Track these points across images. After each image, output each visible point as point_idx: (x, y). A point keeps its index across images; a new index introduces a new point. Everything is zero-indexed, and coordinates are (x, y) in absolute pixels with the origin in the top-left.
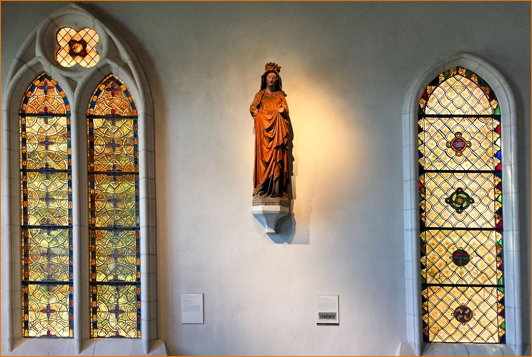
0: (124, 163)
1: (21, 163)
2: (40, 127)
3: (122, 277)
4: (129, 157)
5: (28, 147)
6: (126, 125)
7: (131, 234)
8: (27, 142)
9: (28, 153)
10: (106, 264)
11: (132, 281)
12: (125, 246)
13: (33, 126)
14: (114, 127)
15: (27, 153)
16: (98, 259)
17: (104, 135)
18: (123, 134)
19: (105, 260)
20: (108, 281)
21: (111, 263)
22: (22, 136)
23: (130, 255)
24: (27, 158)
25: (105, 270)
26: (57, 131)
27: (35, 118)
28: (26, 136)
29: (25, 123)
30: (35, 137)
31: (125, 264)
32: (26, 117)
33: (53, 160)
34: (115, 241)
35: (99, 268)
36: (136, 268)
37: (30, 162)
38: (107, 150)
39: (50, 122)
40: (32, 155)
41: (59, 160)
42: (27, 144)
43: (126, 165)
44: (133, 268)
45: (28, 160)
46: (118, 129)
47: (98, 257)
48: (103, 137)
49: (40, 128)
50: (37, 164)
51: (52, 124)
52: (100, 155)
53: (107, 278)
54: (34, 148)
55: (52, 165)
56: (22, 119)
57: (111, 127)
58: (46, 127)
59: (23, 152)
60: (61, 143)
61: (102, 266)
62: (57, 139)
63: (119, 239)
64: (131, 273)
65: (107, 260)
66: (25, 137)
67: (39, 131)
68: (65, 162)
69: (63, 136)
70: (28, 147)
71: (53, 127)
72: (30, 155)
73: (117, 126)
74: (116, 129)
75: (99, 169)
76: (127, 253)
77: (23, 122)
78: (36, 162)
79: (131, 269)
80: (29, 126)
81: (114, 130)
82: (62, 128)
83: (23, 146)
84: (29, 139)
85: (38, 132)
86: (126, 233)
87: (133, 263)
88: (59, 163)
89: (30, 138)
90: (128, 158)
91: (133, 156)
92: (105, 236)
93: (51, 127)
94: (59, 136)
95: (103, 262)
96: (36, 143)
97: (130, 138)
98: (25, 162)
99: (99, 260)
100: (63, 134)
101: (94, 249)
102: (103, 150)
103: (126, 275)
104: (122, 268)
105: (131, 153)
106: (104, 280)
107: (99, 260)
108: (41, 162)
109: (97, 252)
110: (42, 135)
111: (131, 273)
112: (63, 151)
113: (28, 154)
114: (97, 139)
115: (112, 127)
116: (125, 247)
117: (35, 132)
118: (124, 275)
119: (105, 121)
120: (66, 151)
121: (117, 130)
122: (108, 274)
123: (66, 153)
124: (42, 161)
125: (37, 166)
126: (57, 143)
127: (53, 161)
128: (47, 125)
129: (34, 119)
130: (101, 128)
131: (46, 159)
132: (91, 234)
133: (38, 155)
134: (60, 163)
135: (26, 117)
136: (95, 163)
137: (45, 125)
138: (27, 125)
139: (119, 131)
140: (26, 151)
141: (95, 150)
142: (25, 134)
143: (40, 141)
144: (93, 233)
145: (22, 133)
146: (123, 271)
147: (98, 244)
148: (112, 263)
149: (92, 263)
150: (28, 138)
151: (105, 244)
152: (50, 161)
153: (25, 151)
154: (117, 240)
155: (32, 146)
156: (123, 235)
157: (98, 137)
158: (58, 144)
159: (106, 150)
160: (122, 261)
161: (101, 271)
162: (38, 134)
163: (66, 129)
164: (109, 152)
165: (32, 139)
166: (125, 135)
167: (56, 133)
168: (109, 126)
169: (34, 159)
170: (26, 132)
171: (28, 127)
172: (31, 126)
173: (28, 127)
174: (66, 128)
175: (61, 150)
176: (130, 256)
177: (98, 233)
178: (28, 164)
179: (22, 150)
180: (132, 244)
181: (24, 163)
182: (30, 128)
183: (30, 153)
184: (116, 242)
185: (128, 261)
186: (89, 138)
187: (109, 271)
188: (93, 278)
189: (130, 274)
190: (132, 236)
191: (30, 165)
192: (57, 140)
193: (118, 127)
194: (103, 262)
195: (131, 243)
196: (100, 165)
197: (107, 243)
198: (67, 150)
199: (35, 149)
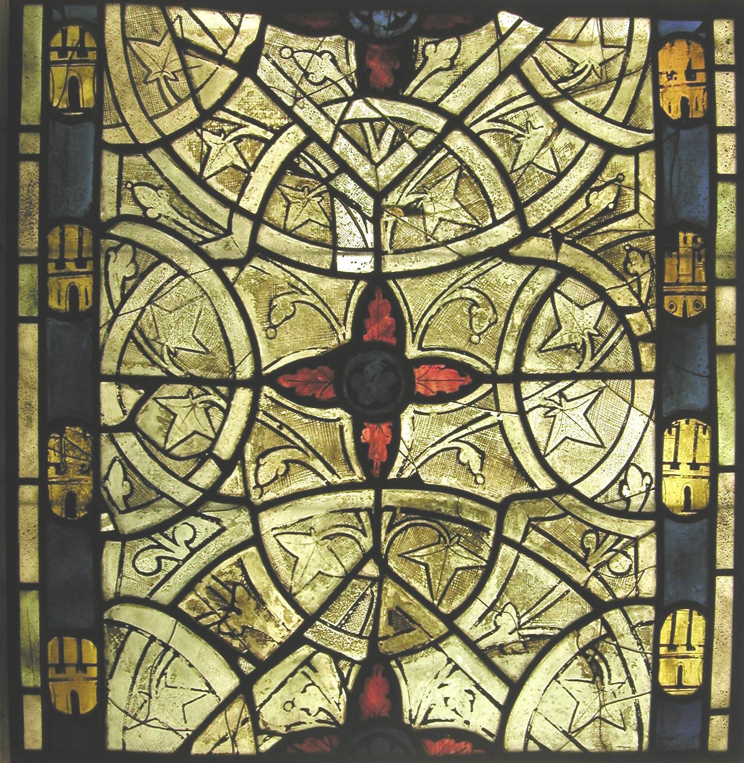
3: (457, 685)
7: (591, 56)
10: (242, 502)
11: (590, 745)
12: (508, 231)
16: (130, 425)
19: (225, 448)
20: (267, 745)
21: (309, 481)
23: (569, 365)
25: (231, 586)
31: (503, 508)
34: (364, 170)
35: (147, 563)
36: (648, 551)
44: (621, 564)
47: (131, 396)
53: (255, 715)
61: (183, 532)
63: (422, 140)
64: (589, 633)
65: (264, 438)
76: (536, 339)
79: (580, 576)
86: (517, 44)
87: (621, 480)
92: (234, 87)
95: (207, 475)
99: (144, 438)
101: (84, 284)
103: (514, 665)
104: (460, 559)
106: (217, 729)
107: (144, 438)
109: (125, 323)
111: (589, 633)
116: (502, 253)
118: (484, 656)
122: (264, 652)
132: (47, 65)
144: (63, 51)
146: (477, 608)
147: (128, 208)
148: (330, 488)
149: (42, 482)
151: (234, 208)
154: (393, 149)
156: (488, 71)
160: (469, 456)
161: (171, 609)
176: (574, 377)
177: (130, 56)
180: (603, 199)
184: (387, 172)
185: (541, 458)
187: (277, 605)
188: (62, 705)
189: (564, 651)
190: (604, 95)
194: (207, 475)
195: (587, 186)
197: (251, 203)
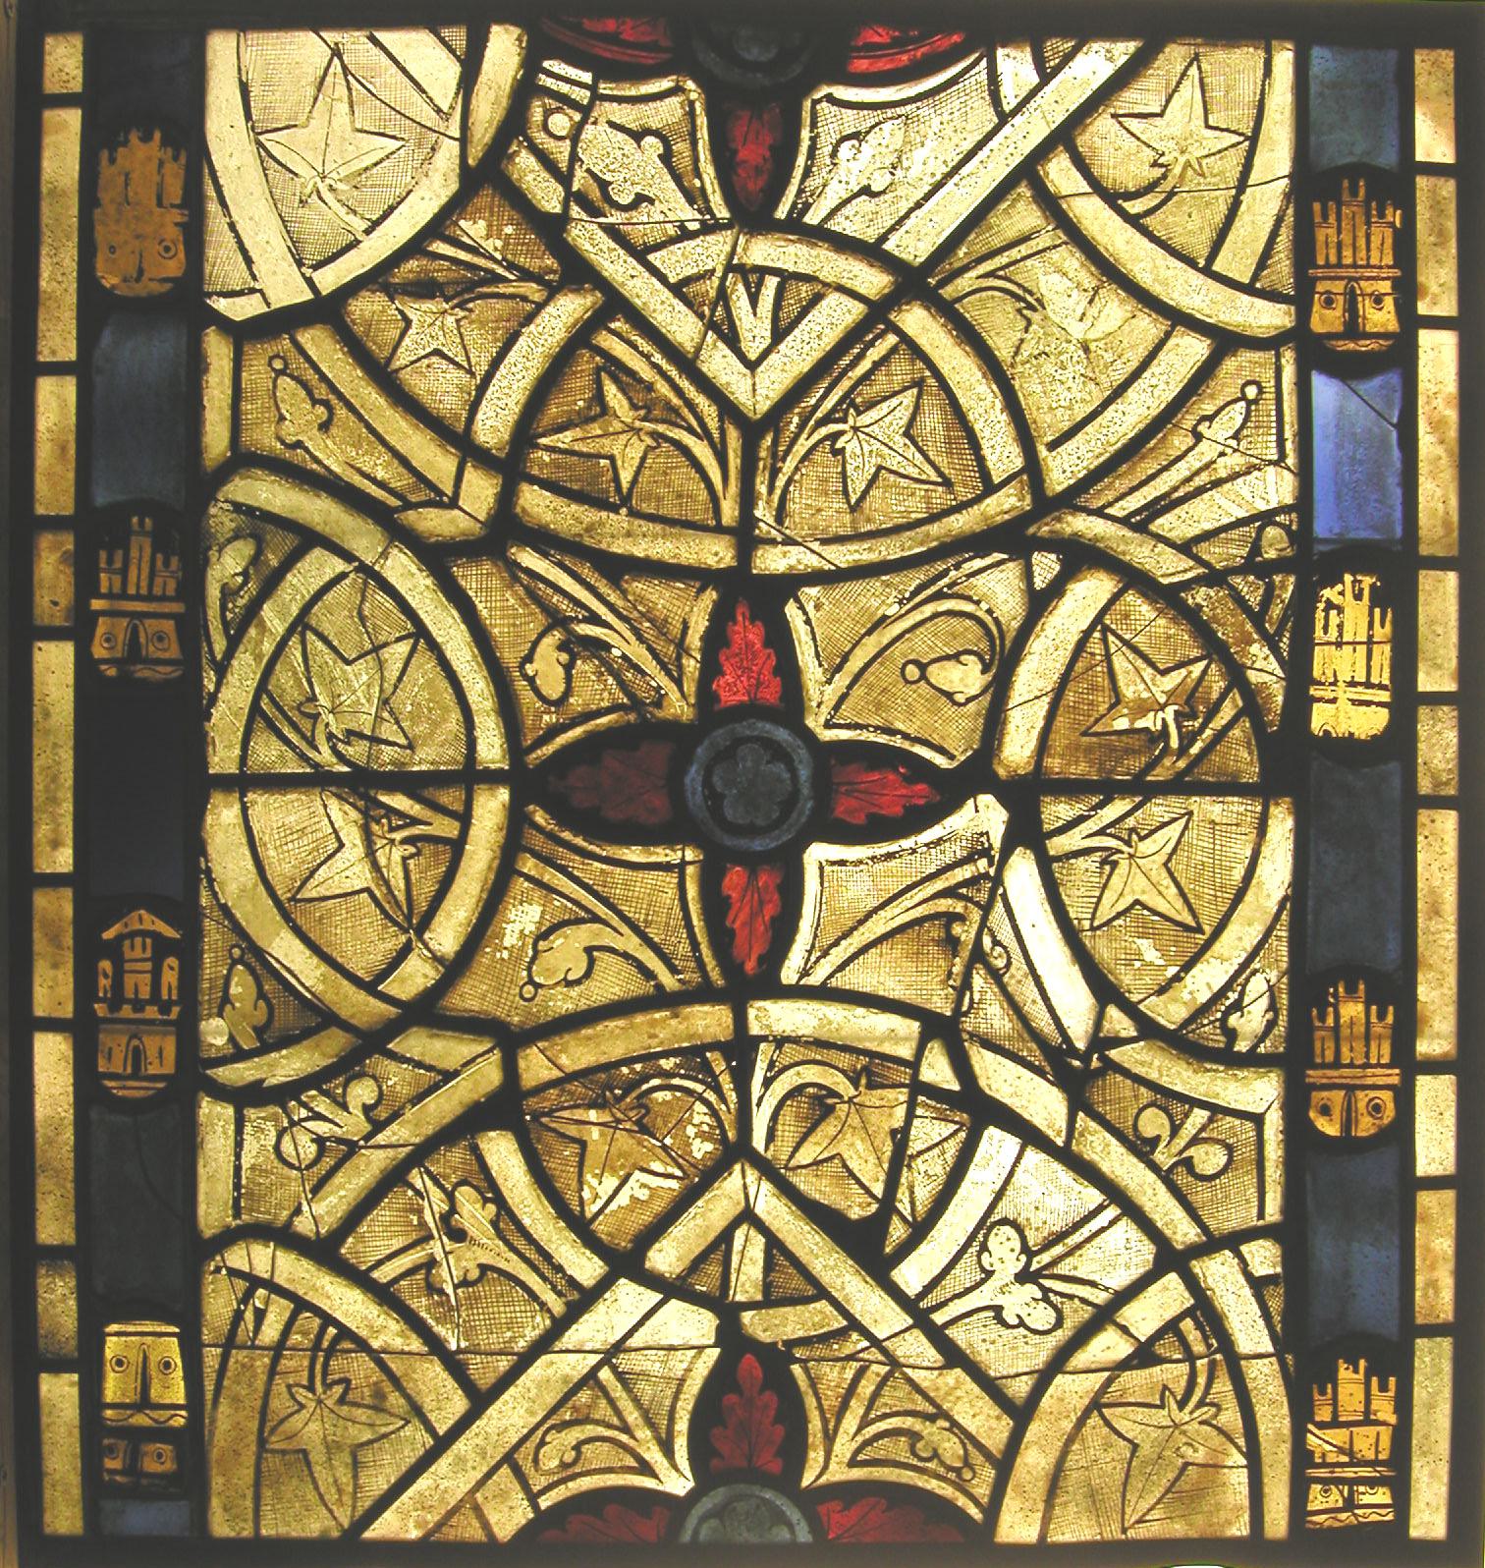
0: (1020, 1301)
4: (1153, 1123)
6: (1112, 198)
14: (762, 251)
17: (480, 492)
18: (1003, 455)
38: (568, 947)
43: (1058, 1363)
46: (878, 314)
48: (437, 557)
52: (362, 1092)
57: (676, 262)
73: (854, 224)
74: (835, 316)
75: (332, 1474)
81: (754, 328)
90: (1142, 1148)
91: (1261, 1092)
97: (1215, 578)
102: (447, 935)
105: (1227, 999)
114: (301, 624)
115: (711, 251)
119: (525, 90)
121: (855, 337)
130: (424, 289)
136: (218, 1302)
139: (902, 369)
141: (214, 934)
157: (319, 567)
159: (522, 918)
164: (613, 983)
166: (1062, 469)
168: (645, 225)
186: (85, 585)
193: (872, 252)
196: (360, 1369)
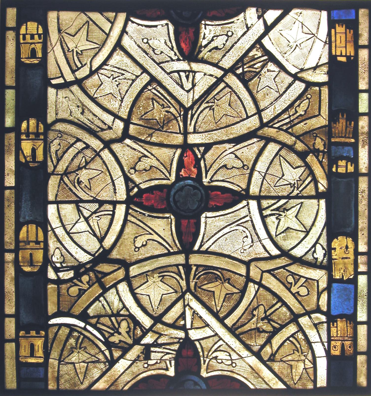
1: (10, 348)
2: (146, 78)
5: (60, 232)
8: (51, 197)
9: (57, 270)
13: (92, 73)
15: (51, 275)
22: (18, 149)
24: (52, 308)
26: (259, 112)
27: (111, 15)
28: (46, 150)
29: (40, 55)
30: (106, 154)
32: (52, 16)
33: (229, 322)
37: (72, 341)
39: (219, 42)
40: (82, 292)
41: (267, 318)
42: (52, 209)
45: (60, 325)
49: (145, 87)
50: (117, 354)
51: (227, 63)
54: (101, 240)
55: (221, 355)
56: (23, 31)
58: (188, 86)
59: (27, 269)
60: (289, 197)
62: (261, 166)
66: (40, 156)
67: (139, 111)
68: (313, 335)
69: (300, 146)
70: (60, 232)
71: (232, 80)
72: (74, 291)
77: (25, 51)
78: (115, 339)
80: (70, 77)
82: (299, 87)
83: (28, 223)
84: (66, 173)
85: (127, 122)
88: (269, 341)
89: (76, 162)
93: (220, 80)
94: (272, 148)
96: (114, 203)
98: (39, 343)
100: (300, 128)
108: (149, 339)
110: (154, 139)
112: (298, 252)
113: (59, 282)
117: (108, 119)
120: (320, 254)
123: (320, 267)
124: (150, 329)
125: (121, 366)
126: (259, 198)
127: (232, 330)
128: (195, 66)
129: (107, 26)
131: (183, 316)
133: (123, 287)
134: (277, 341)
135: (52, 16)
137: (183, 65)
138: (52, 70)
140: (47, 260)
142: (37, 134)
143: (143, 186)
145: (16, 129)
150: (61, 167)
152: (208, 332)
153: (39, 256)
155: (82, 226)
158: (265, 203)
162: (132, 129)
163: (325, 91)
165: (84, 175)
167: (254, 122)
169: (99, 316)
170: (50, 120)
171: (58, 87)
172: (80, 74)
173: (61, 81)
174: (320, 85)
175: (285, 253)
178: (55, 354)
179: (16, 251)
181: (32, 346)
182: (75, 88)
183: (71, 274)
191: (74, 358)
192: (256, 178)
198: (329, 251)
199: (108, 242)
